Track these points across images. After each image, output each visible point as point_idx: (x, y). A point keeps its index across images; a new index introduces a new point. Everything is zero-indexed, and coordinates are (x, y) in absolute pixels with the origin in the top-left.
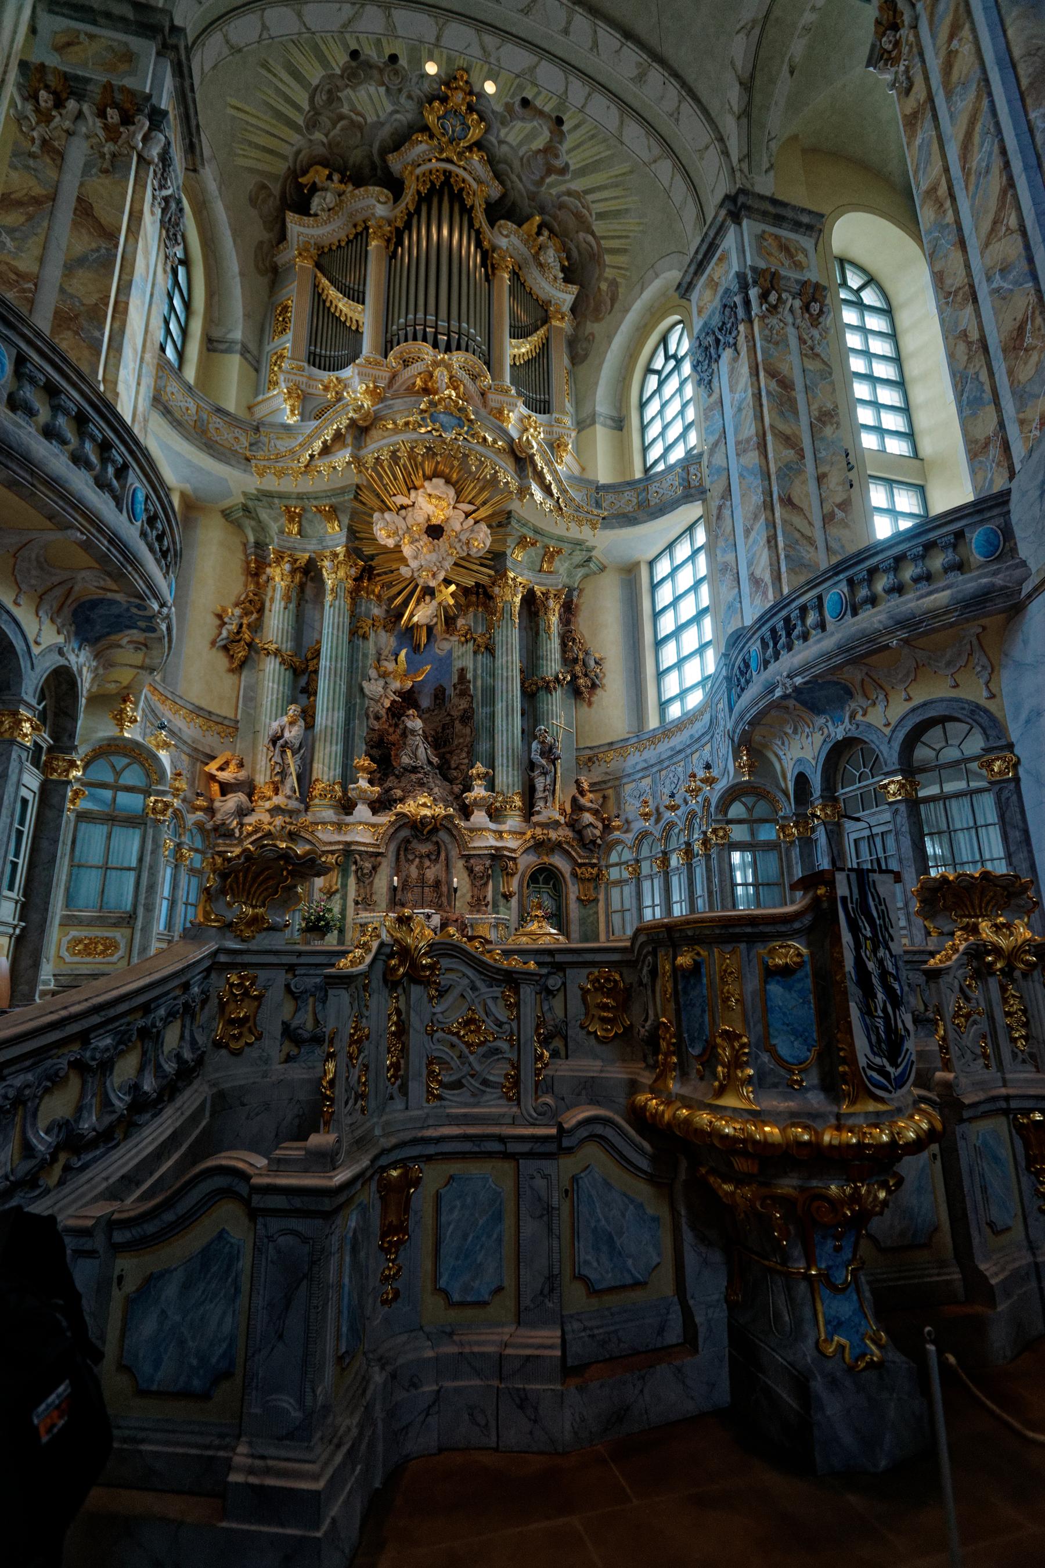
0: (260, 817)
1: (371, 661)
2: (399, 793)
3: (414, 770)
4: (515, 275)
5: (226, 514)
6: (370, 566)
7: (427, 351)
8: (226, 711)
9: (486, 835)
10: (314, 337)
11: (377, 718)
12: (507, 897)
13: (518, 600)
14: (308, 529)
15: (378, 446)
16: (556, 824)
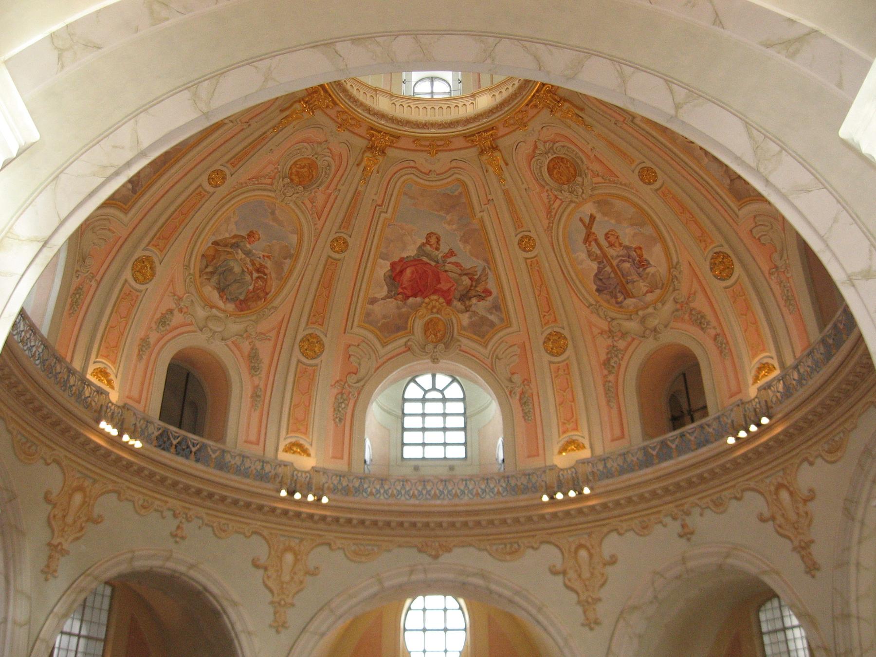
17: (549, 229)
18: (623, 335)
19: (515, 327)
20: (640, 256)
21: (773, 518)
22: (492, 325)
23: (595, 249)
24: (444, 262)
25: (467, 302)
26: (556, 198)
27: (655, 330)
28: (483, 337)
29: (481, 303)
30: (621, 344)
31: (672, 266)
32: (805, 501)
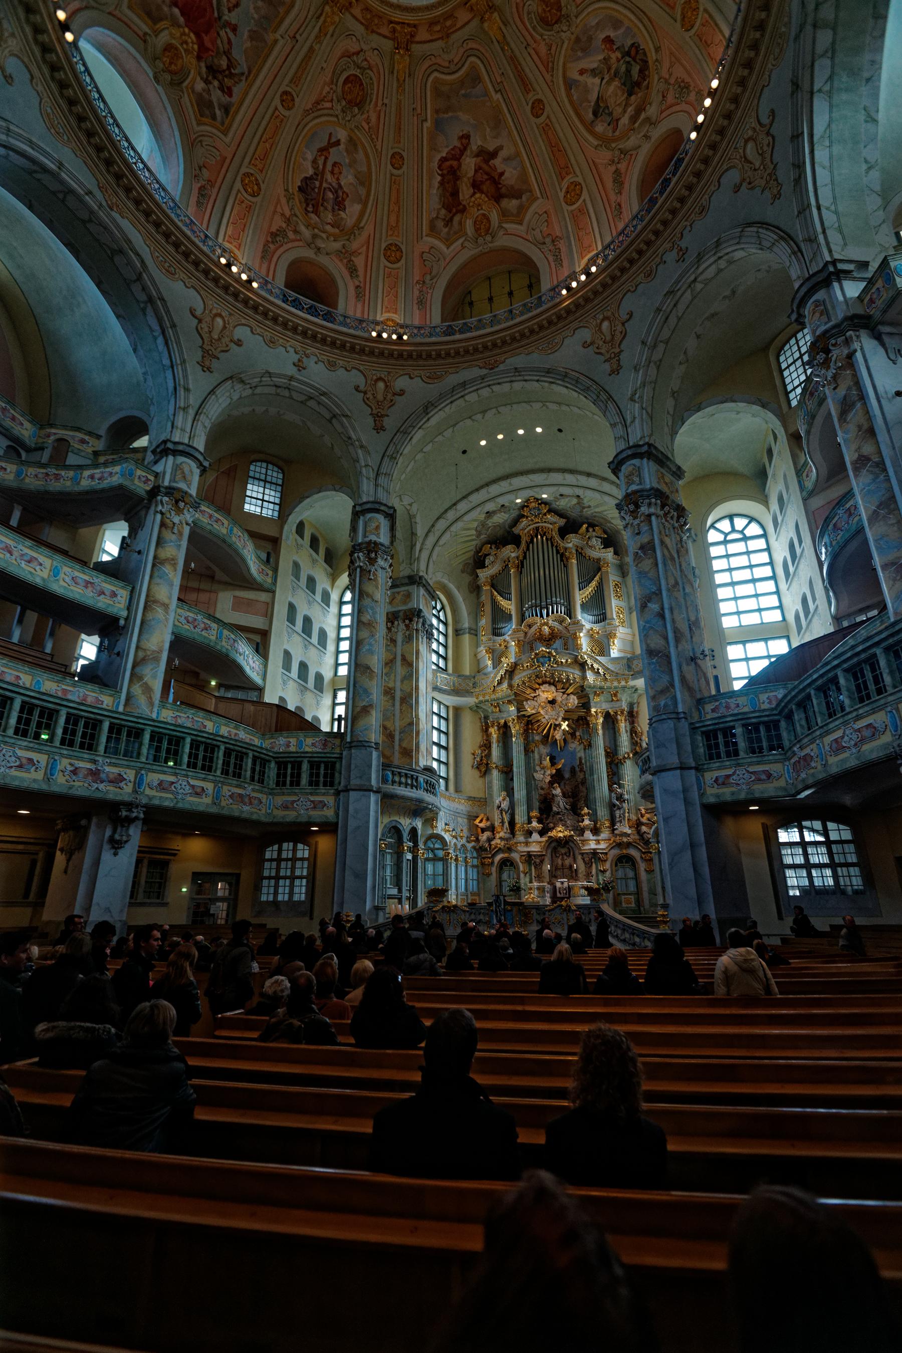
0: (497, 842)
1: (537, 762)
2: (552, 825)
3: (558, 813)
4: (580, 554)
5: (471, 708)
6: (529, 722)
7: (538, 619)
8: (481, 795)
9: (592, 843)
10: (494, 620)
11: (542, 789)
12: (604, 872)
13: (601, 720)
14: (503, 709)
15: (517, 680)
16: (627, 835)
17: (307, 112)
18: (296, 232)
19: (227, 140)
20: (344, 200)
21: (365, 393)
22: (214, 117)
23: (321, 162)
24: (224, 26)
25: (210, 78)
26: (332, 101)
27: (319, 249)
28: (201, 116)
29: (219, 93)
30: (291, 235)
31: (358, 226)
32: (394, 394)
